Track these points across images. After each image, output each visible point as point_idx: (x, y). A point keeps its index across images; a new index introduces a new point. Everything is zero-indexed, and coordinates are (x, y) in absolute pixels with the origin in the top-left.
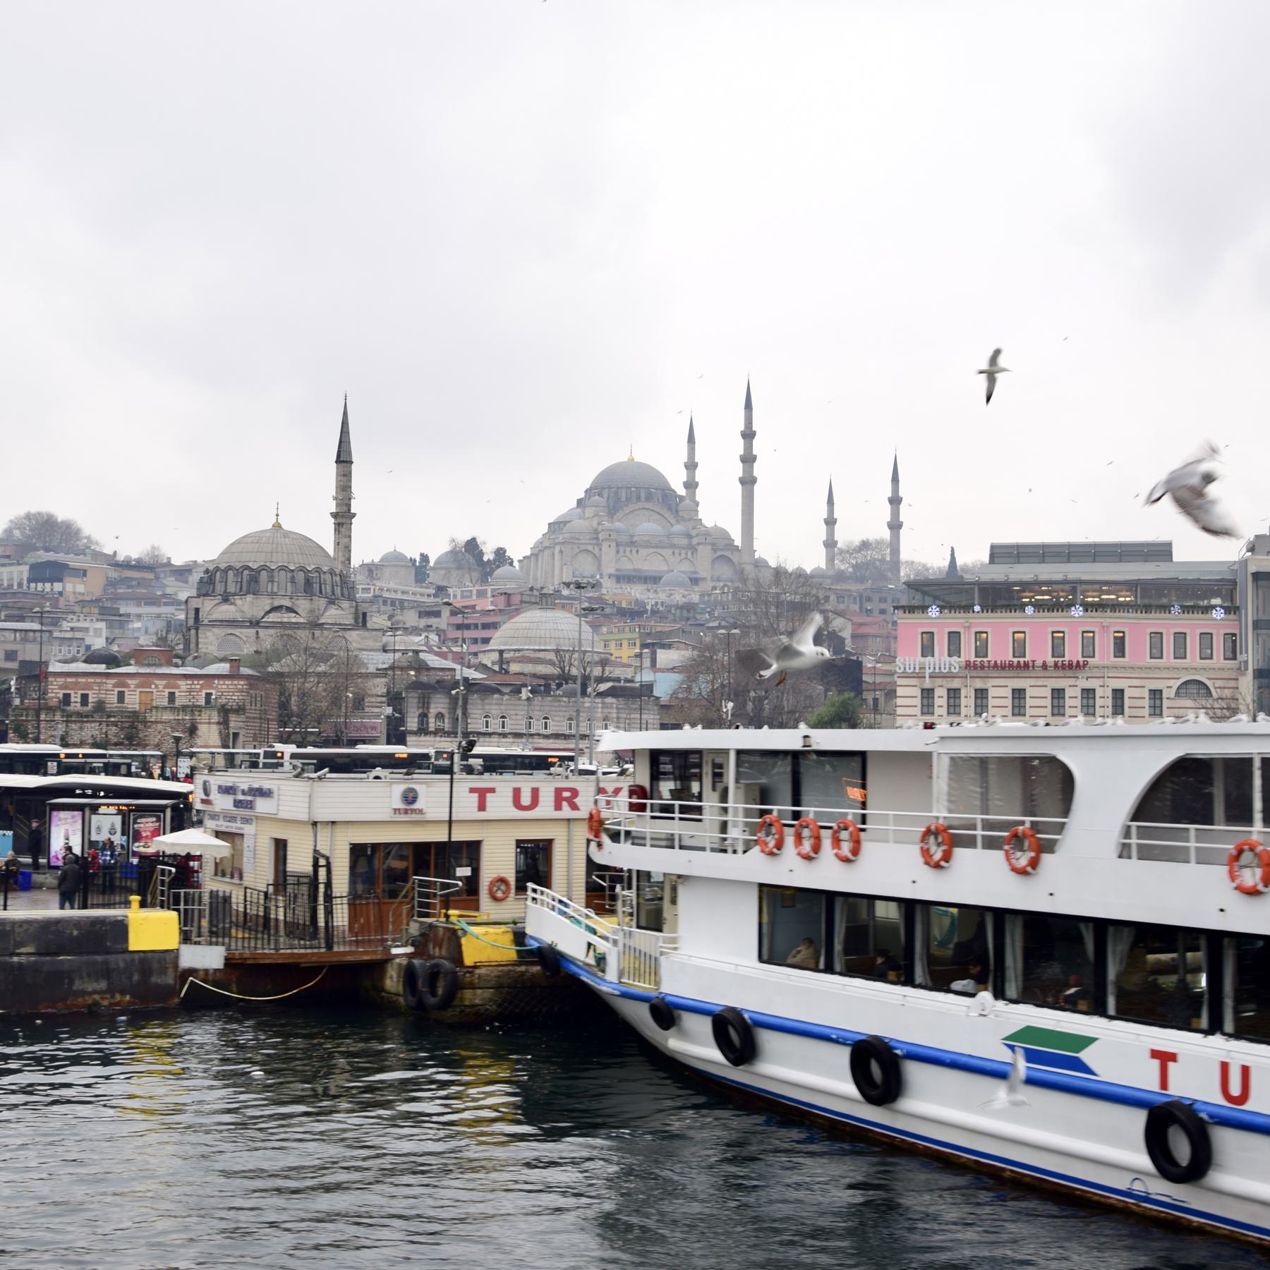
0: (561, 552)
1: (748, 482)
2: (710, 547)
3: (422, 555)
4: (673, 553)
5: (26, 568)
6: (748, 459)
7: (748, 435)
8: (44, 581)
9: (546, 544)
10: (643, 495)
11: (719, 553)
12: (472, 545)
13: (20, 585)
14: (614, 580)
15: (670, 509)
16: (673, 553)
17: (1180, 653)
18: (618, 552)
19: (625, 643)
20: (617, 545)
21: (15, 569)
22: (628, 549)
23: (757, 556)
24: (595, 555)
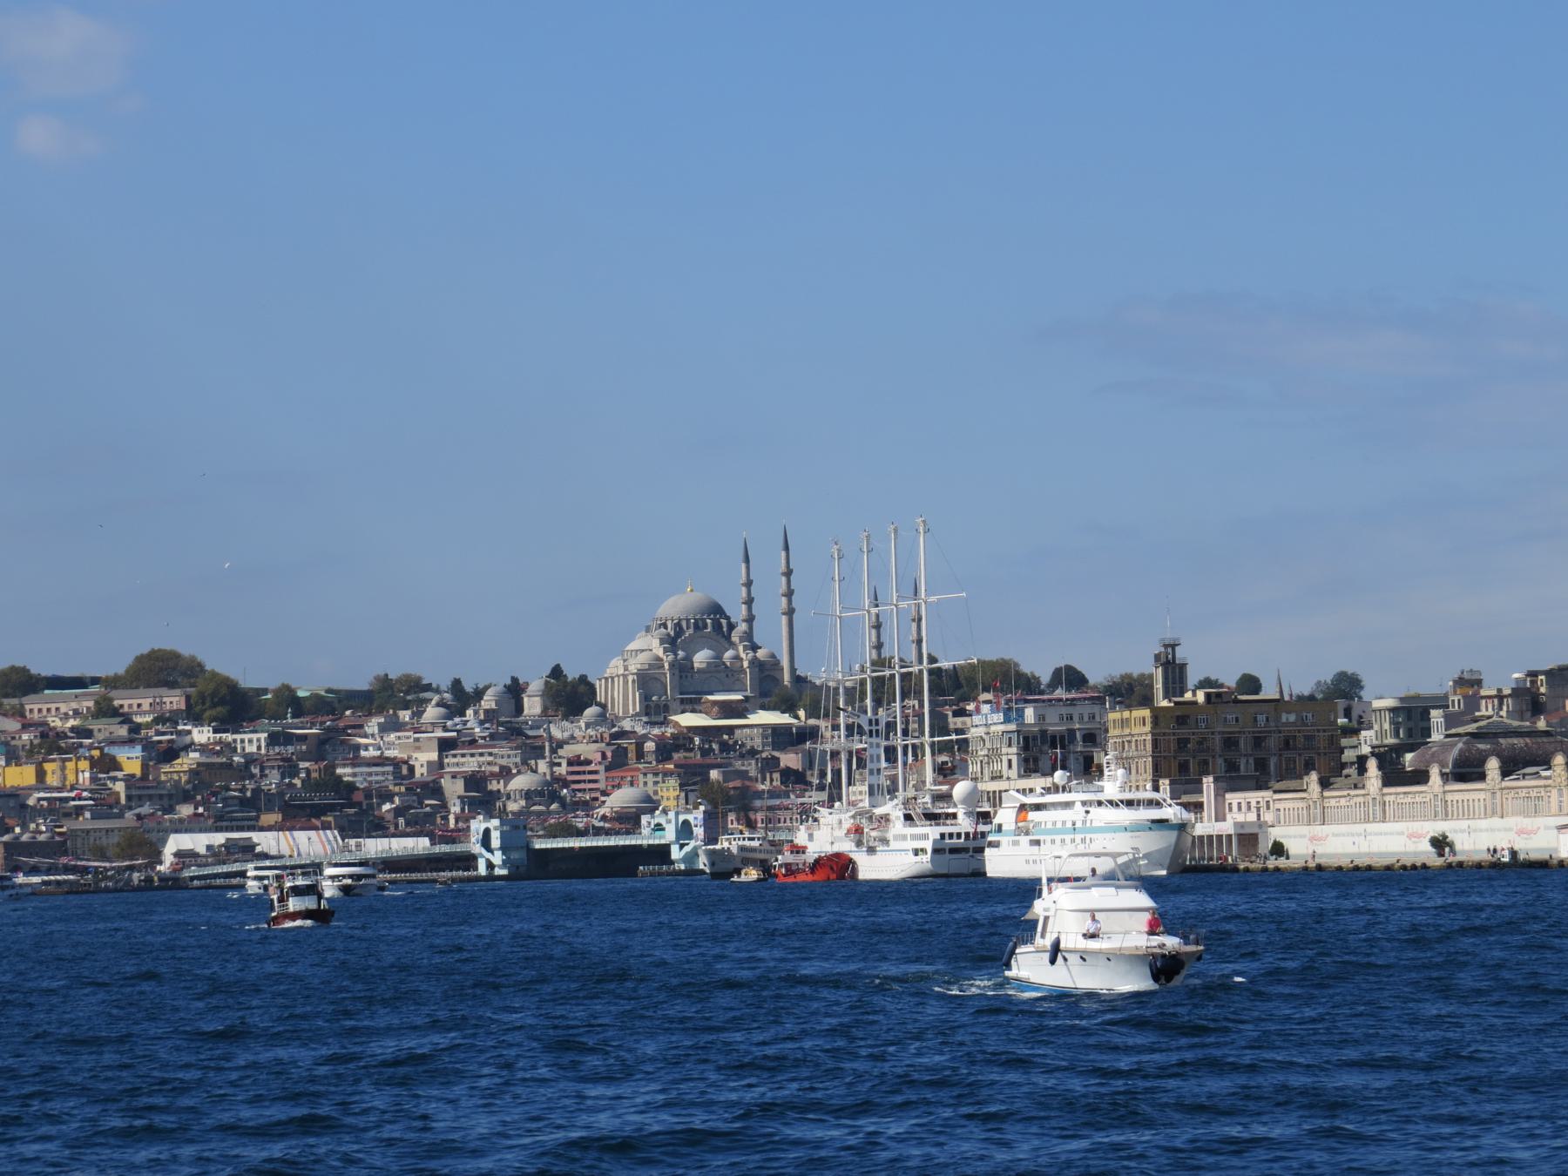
0: (633, 681)
1: (790, 612)
2: (757, 669)
3: (515, 680)
4: (727, 676)
5: (263, 736)
6: (789, 594)
7: (788, 573)
8: (279, 745)
9: (621, 671)
10: (700, 624)
11: (767, 673)
12: (557, 672)
13: (259, 748)
14: (678, 702)
15: (724, 636)
16: (727, 676)
17: (785, 822)
18: (681, 677)
19: (671, 789)
20: (680, 672)
21: (255, 736)
22: (689, 675)
23: (798, 673)
24: (662, 682)
